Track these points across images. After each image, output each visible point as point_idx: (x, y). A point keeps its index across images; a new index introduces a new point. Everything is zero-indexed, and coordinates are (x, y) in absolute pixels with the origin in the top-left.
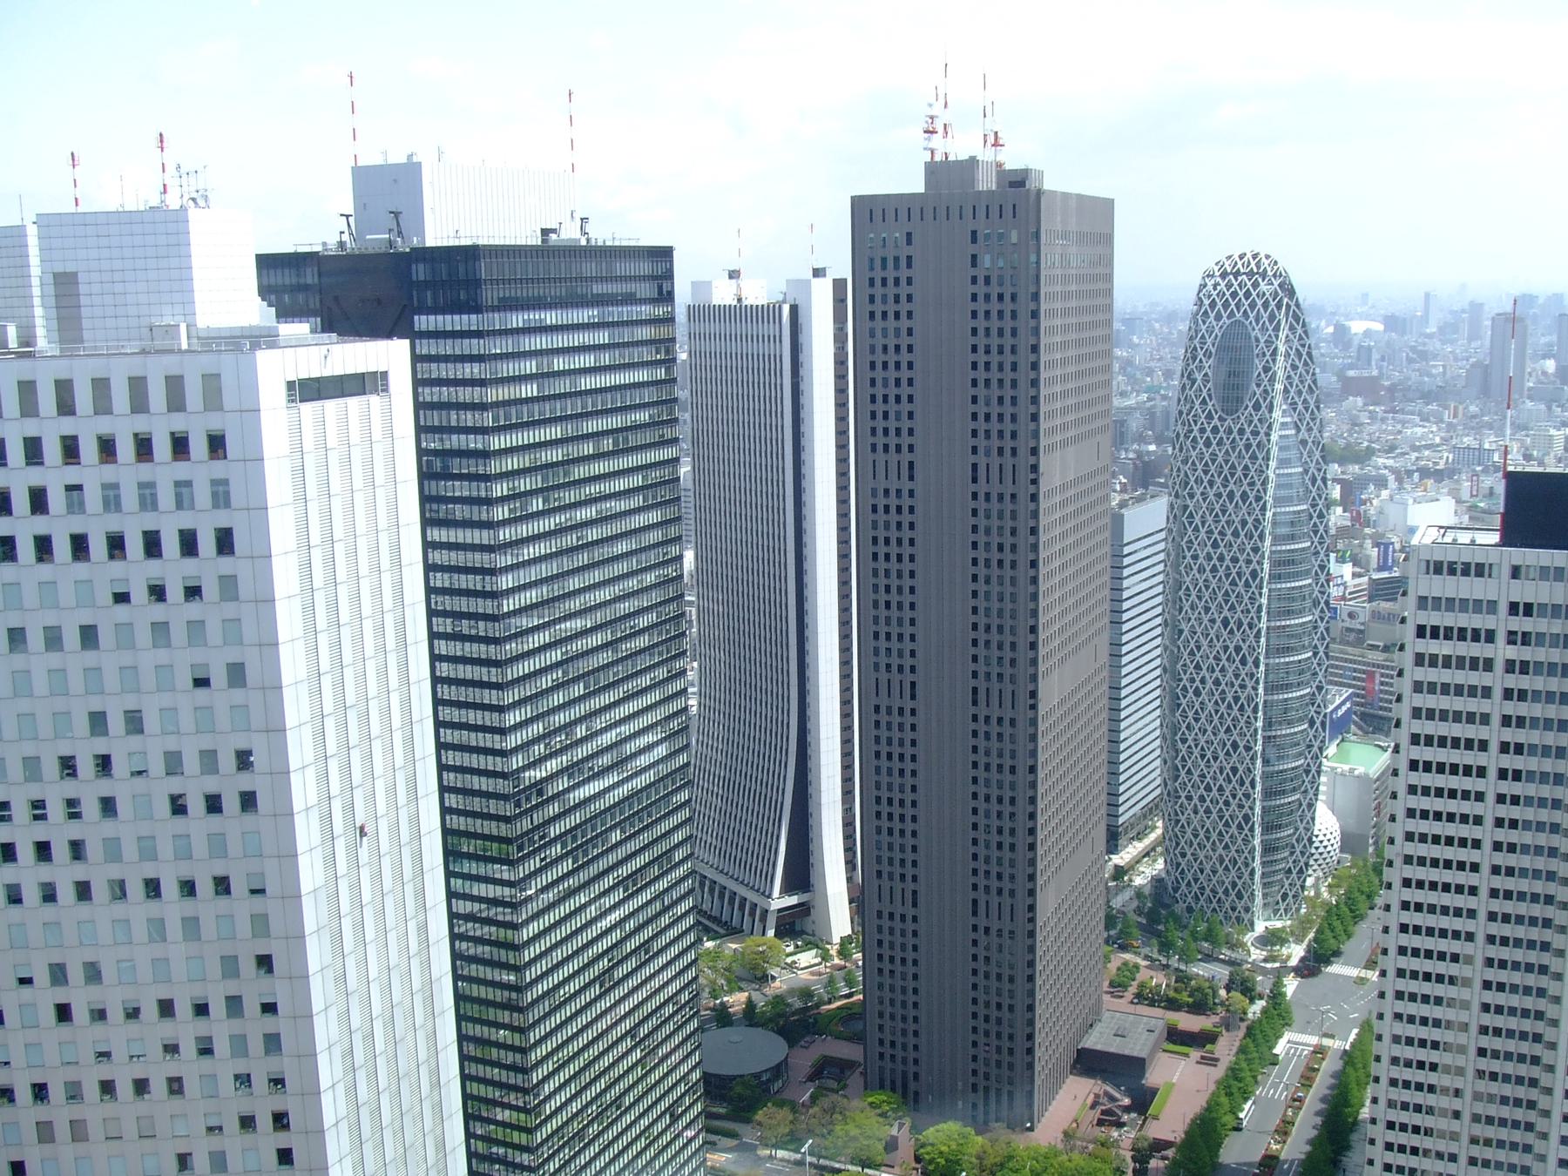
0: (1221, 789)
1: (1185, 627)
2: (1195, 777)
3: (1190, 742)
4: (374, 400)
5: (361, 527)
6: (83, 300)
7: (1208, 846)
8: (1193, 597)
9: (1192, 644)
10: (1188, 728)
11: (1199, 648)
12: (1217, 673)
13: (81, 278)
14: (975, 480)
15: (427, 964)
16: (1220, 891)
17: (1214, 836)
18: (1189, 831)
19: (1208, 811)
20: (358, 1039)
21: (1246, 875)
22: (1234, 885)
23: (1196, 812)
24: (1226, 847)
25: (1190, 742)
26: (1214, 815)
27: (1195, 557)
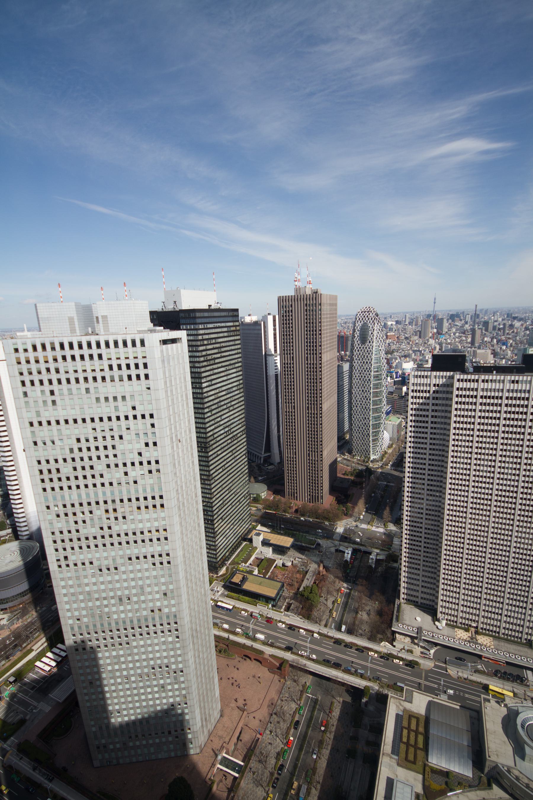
4: (178, 345)
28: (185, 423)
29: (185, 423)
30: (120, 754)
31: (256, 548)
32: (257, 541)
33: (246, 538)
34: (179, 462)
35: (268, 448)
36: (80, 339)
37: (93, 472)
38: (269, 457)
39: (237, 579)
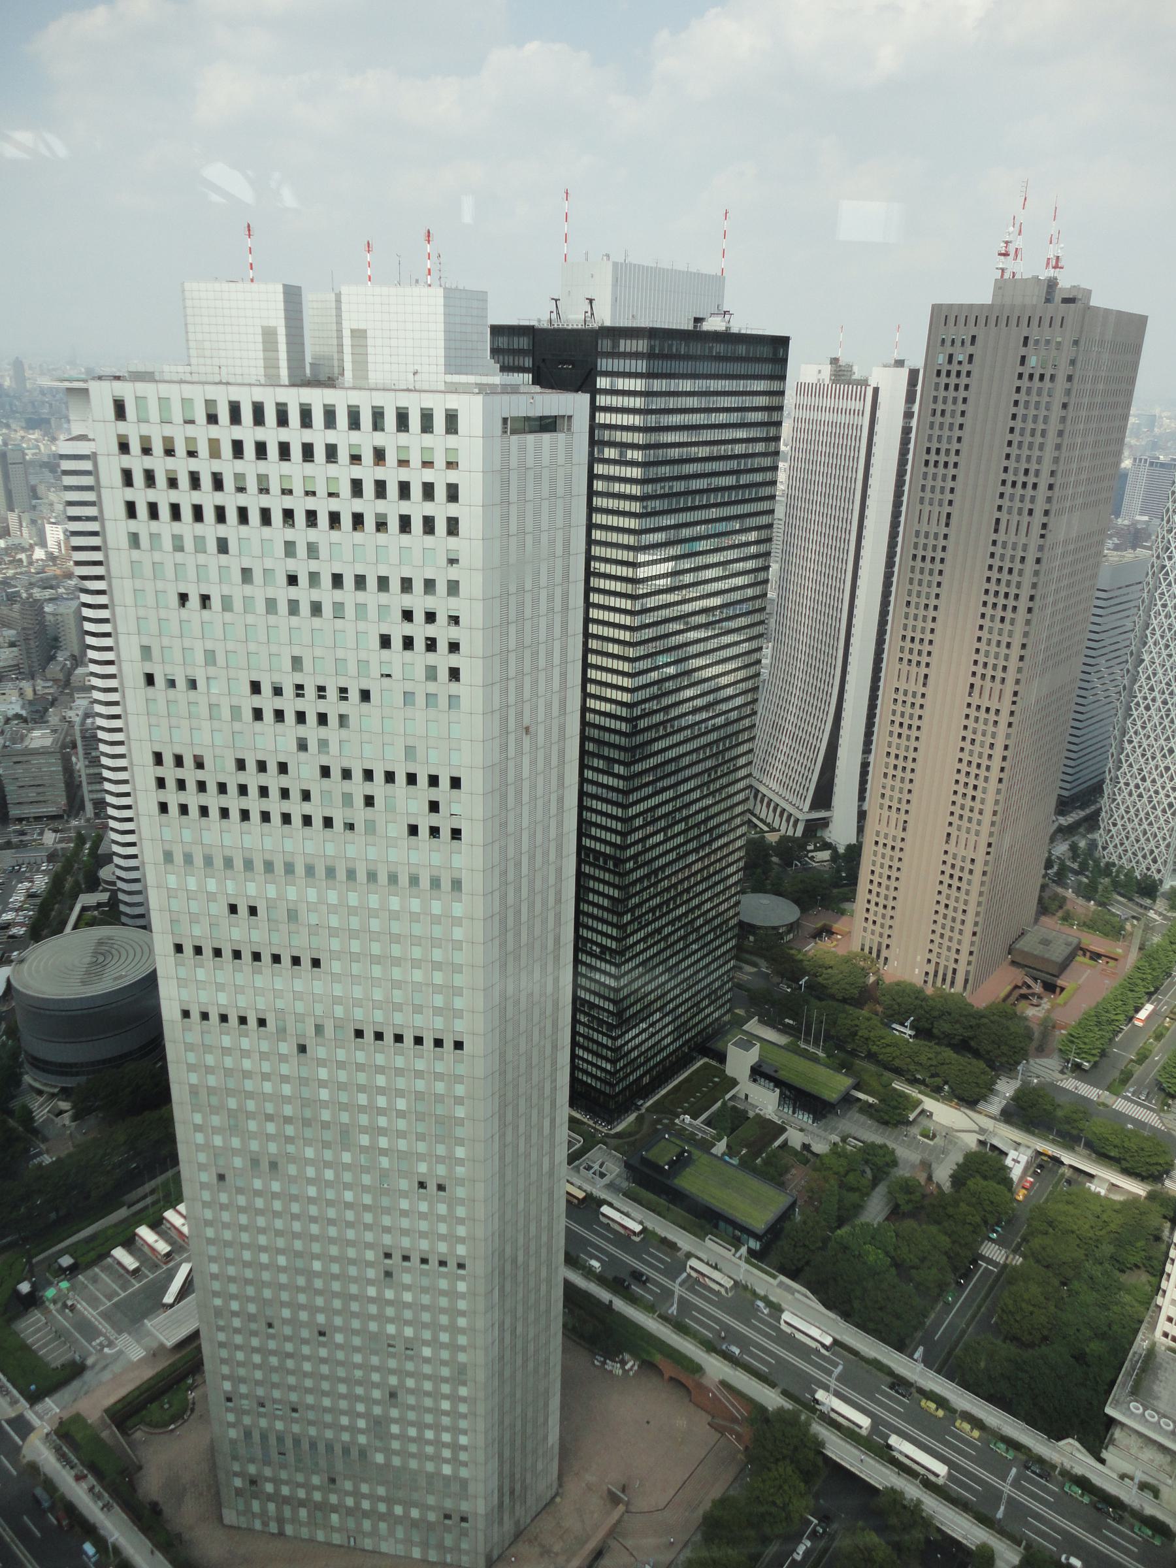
0: (1154, 781)
1: (1145, 657)
2: (1135, 770)
3: (1135, 744)
4: (561, 437)
5: (545, 525)
6: (370, 350)
7: (1136, 821)
8: (1158, 636)
9: (1150, 671)
10: (1136, 733)
11: (1155, 674)
12: (1167, 696)
13: (369, 334)
14: (996, 531)
15: (560, 824)
16: (1140, 855)
17: (1142, 815)
18: (1122, 808)
19: (1140, 796)
20: (511, 865)
21: (1163, 847)
22: (1152, 852)
23: (1130, 794)
24: (1151, 824)
25: (1135, 744)
26: (1145, 799)
27: (1164, 606)
28: (549, 679)
29: (549, 679)
30: (287, 1512)
31: (734, 1083)
32: (739, 1062)
33: (708, 1045)
34: (519, 793)
35: (823, 797)
36: (259, 395)
37: (284, 781)
38: (825, 823)
39: (663, 1154)
